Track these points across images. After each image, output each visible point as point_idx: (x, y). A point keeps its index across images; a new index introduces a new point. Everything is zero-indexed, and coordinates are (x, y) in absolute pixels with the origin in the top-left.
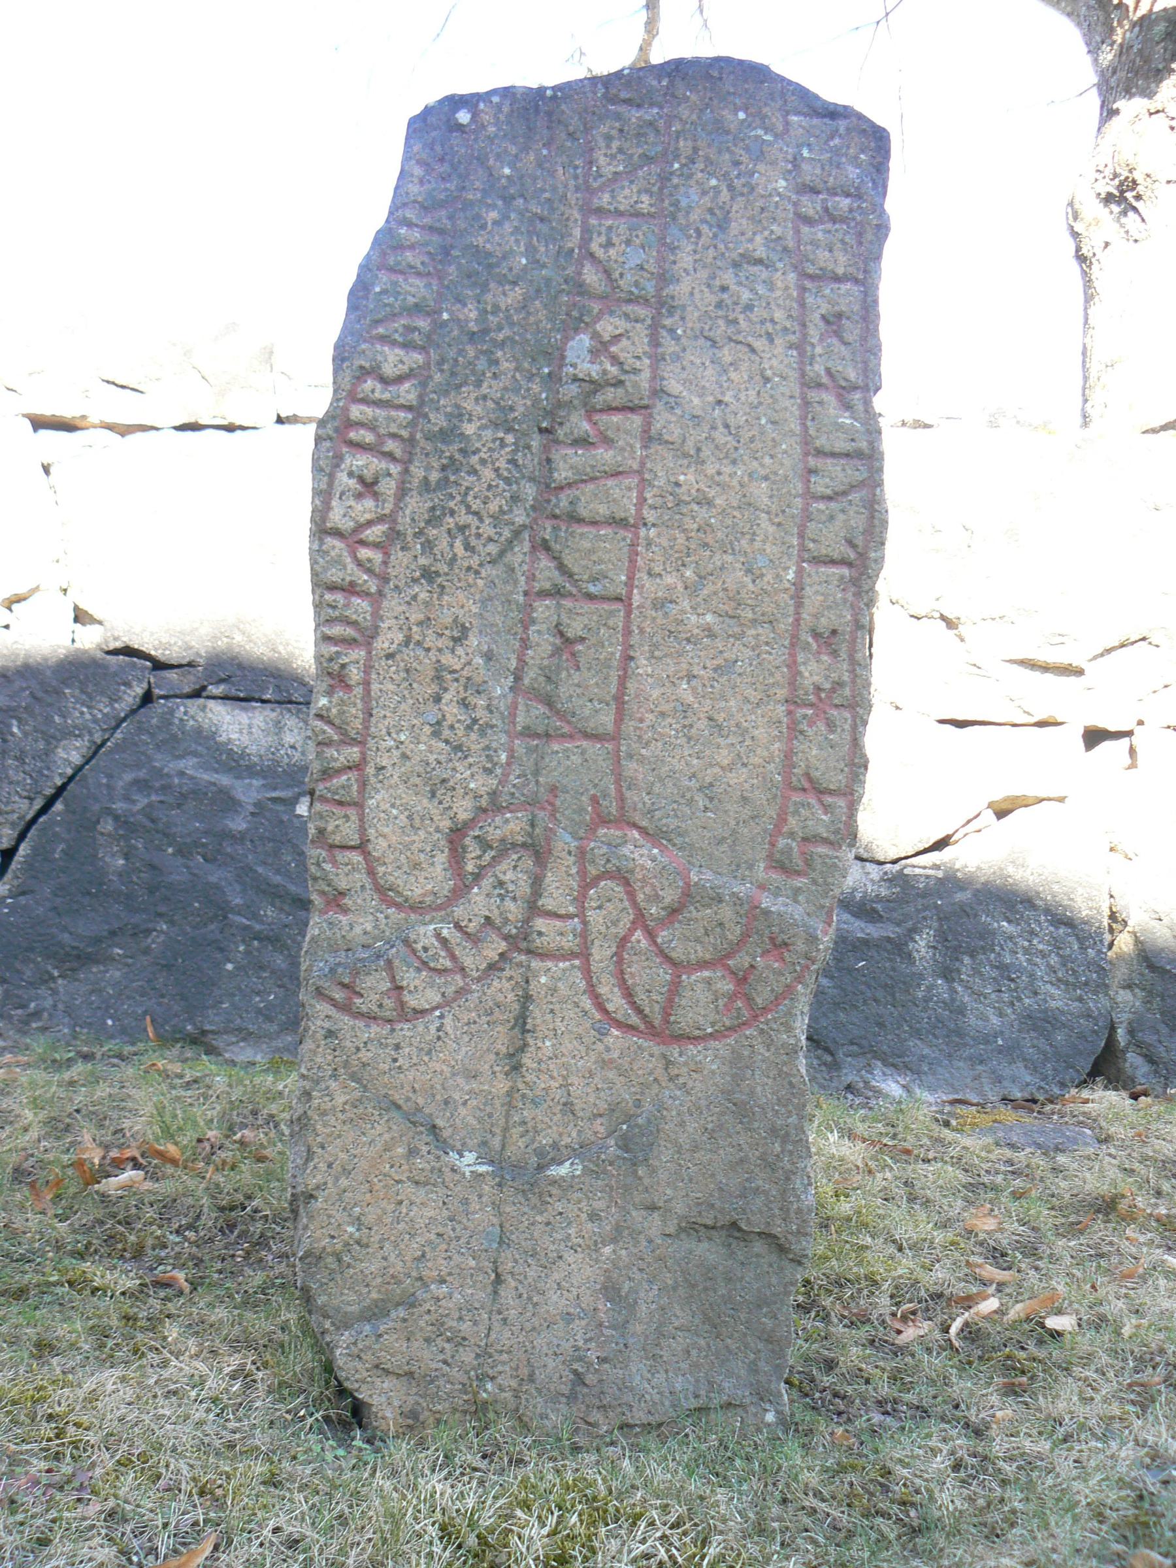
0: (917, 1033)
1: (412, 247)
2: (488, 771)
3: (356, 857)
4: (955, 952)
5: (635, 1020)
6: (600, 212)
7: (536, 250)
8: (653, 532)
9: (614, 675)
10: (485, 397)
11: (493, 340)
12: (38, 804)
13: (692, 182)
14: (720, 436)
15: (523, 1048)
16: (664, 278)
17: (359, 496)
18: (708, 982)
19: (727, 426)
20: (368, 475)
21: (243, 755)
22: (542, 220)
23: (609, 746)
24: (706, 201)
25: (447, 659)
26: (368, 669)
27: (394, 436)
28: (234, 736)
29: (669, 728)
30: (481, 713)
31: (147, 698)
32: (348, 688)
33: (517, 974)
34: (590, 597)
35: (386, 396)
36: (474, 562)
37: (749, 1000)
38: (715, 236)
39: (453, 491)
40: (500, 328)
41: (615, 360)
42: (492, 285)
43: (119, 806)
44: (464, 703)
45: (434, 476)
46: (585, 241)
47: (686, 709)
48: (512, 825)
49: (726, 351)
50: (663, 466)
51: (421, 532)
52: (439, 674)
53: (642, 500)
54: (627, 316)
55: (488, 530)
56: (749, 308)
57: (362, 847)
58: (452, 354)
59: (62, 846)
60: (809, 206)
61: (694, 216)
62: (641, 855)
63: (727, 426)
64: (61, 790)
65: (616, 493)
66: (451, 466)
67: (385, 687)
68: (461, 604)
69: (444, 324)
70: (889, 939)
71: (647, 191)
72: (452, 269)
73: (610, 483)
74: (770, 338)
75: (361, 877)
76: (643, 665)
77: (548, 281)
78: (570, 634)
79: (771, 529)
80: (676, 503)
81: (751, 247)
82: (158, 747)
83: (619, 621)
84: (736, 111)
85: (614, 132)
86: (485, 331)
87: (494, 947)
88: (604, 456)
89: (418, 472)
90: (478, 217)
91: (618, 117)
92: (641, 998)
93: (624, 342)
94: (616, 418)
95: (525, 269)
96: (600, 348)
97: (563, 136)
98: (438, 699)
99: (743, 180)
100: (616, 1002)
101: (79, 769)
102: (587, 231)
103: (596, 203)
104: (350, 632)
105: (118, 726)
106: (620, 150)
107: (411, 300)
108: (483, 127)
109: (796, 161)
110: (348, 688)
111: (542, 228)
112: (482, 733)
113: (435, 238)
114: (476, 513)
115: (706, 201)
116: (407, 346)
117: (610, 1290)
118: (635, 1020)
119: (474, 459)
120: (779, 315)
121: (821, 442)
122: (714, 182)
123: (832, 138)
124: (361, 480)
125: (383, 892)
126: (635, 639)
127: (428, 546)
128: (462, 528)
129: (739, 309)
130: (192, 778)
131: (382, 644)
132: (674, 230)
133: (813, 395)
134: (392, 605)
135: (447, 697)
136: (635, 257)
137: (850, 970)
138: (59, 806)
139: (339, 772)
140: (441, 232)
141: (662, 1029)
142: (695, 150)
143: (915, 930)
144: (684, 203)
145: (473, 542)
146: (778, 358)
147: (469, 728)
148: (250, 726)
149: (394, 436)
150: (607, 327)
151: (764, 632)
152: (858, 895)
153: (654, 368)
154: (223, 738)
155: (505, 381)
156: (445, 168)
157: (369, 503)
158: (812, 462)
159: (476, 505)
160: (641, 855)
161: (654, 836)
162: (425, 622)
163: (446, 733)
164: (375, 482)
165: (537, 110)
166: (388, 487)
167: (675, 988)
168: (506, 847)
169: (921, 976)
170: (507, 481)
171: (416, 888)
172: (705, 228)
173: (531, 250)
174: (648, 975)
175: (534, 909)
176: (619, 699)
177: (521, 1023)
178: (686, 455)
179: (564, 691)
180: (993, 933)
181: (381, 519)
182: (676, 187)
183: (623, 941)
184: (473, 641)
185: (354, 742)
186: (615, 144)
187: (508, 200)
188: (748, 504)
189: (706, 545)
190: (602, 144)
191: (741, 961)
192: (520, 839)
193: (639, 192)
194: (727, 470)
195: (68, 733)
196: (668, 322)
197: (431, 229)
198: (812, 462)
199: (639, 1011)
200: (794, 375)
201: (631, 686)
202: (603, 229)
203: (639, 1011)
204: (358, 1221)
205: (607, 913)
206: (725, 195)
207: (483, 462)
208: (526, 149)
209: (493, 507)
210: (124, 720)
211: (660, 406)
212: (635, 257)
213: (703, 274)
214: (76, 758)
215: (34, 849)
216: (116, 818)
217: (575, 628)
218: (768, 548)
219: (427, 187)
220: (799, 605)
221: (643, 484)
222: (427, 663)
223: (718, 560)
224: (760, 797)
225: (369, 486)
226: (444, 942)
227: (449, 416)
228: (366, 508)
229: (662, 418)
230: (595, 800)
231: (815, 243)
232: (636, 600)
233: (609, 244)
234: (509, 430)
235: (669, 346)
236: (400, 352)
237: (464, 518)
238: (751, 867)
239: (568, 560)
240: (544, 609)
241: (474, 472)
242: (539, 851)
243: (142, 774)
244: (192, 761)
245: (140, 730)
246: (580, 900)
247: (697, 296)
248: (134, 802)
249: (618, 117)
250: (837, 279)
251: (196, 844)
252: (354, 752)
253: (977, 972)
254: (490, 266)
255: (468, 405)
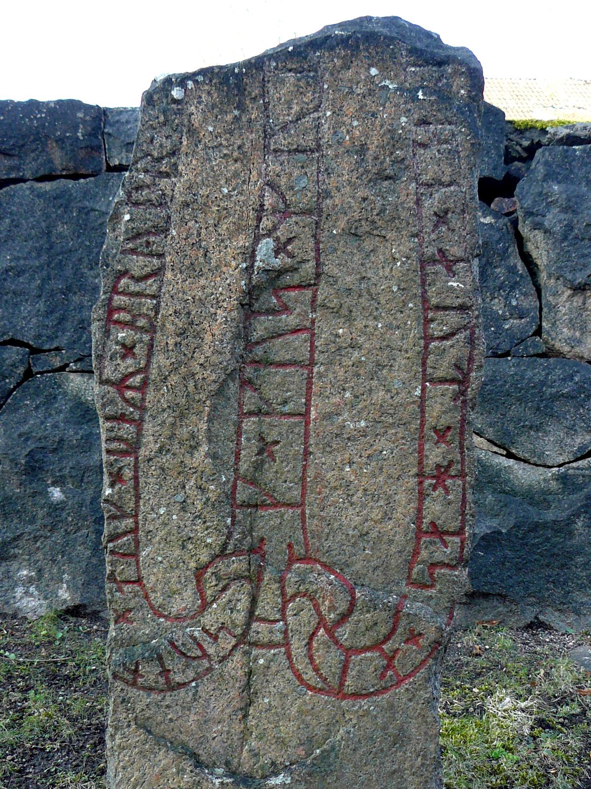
20: (128, 342)
26: (136, 468)
29: (337, 496)
35: (137, 289)
48: (237, 564)
57: (139, 581)
94: (293, 293)
100: (309, 675)
104: (123, 446)
124: (124, 345)
131: (143, 452)
158: (431, 315)
175: (251, 616)
205: (301, 617)
226: (195, 639)
240: (249, 424)
252: (129, 522)
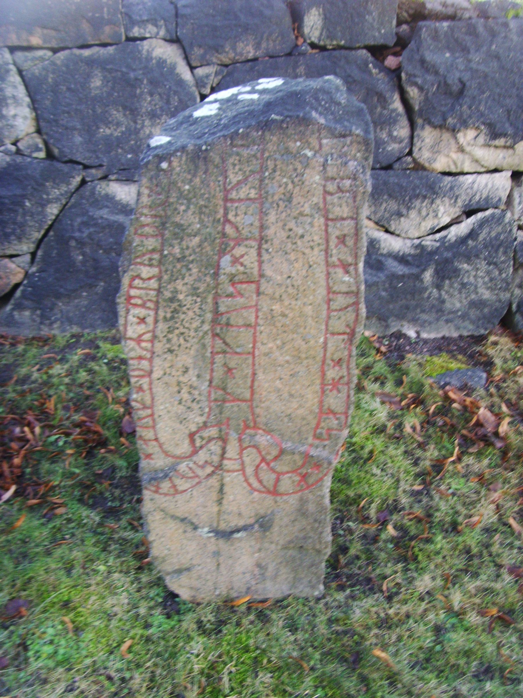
0: (423, 311)
1: (148, 225)
2: (202, 415)
3: (155, 443)
4: (443, 278)
5: (263, 490)
6: (232, 201)
7: (203, 221)
8: (262, 328)
9: (249, 380)
10: (186, 284)
11: (188, 260)
12: (42, 232)
13: (274, 181)
14: (290, 290)
15: (222, 498)
16: (262, 227)
17: (139, 323)
18: (290, 477)
19: (293, 286)
20: (142, 316)
21: (127, 205)
22: (206, 207)
23: (249, 403)
24: (282, 190)
25: (181, 379)
26: (151, 383)
27: (149, 300)
28: (123, 197)
29: (273, 397)
30: (196, 396)
31: (83, 182)
32: (143, 391)
33: (219, 477)
34: (237, 353)
35: (144, 286)
36: (189, 345)
37: (306, 483)
38: (286, 207)
39: (177, 320)
40: (190, 255)
41: (242, 264)
42: (185, 237)
43: (77, 234)
44: (190, 393)
45: (169, 315)
46: (226, 214)
47: (279, 390)
48: (213, 432)
49: (292, 254)
50: (265, 304)
51: (165, 336)
52: (179, 383)
53: (257, 317)
54: (246, 246)
55: (192, 334)
56: (302, 236)
57: (156, 440)
58: (170, 267)
59: (55, 252)
60: (331, 187)
61: (276, 198)
62: (263, 439)
63: (293, 286)
64: (51, 227)
65: (245, 314)
66: (175, 311)
67: (158, 389)
68: (185, 359)
69: (166, 256)
70: (413, 274)
71: (254, 188)
72: (166, 232)
73: (243, 311)
74: (312, 248)
75: (157, 449)
76: (260, 376)
77: (210, 234)
78: (230, 366)
79: (314, 324)
80: (271, 317)
81: (302, 209)
82: (91, 205)
83: (250, 361)
84: (296, 141)
85: (236, 162)
86: (184, 257)
87: (209, 469)
88: (240, 300)
89: (161, 313)
90: (176, 209)
91: (238, 154)
92: (265, 483)
93: (246, 257)
94: (244, 286)
95: (199, 230)
96: (235, 261)
97: (212, 167)
98: (179, 392)
99: (298, 178)
100: (256, 484)
101: (58, 216)
102: (226, 209)
103: (230, 197)
104: (141, 373)
105: (71, 196)
106: (240, 170)
107: (150, 248)
108: (174, 169)
109: (324, 165)
110: (143, 391)
111: (207, 211)
112: (198, 402)
113: (158, 219)
114: (187, 328)
115: (282, 190)
116: (151, 265)
117: (258, 565)
118: (263, 490)
119: (184, 309)
120: (316, 238)
121: (335, 288)
122: (285, 180)
123: (343, 147)
124: (138, 318)
125: (167, 454)
126: (257, 367)
127: (169, 341)
128: (182, 334)
129: (297, 237)
130: (106, 219)
131: (155, 375)
132: (267, 205)
133: (331, 270)
134: (157, 361)
135: (183, 391)
136: (249, 219)
137: (395, 288)
138: (51, 233)
139: (144, 418)
140: (160, 217)
141: (274, 492)
142: (276, 166)
143: (424, 270)
144: (271, 192)
145: (187, 338)
146: (316, 256)
147: (193, 401)
148: (130, 192)
149: (149, 300)
150: (238, 251)
151: (310, 361)
152: (401, 253)
153: (260, 266)
154: (118, 198)
155: (194, 277)
156: (159, 189)
157: (143, 326)
158: (331, 296)
159: (187, 325)
160: (263, 439)
161: (268, 432)
162: (171, 367)
163: (184, 403)
164: (144, 318)
165: (199, 157)
166: (150, 320)
167: (278, 480)
168: (210, 440)
169: (426, 289)
170: (200, 316)
171: (178, 452)
172: (281, 203)
173: (201, 221)
174: (268, 478)
175: (223, 456)
176: (252, 387)
177: (221, 491)
178: (275, 299)
179: (229, 386)
180: (460, 270)
181: (149, 332)
182: (267, 184)
183: (258, 466)
184: (191, 372)
185: (148, 408)
186: (237, 167)
187: (189, 200)
188: (302, 314)
189: (285, 332)
190: (231, 167)
191: (304, 471)
192: (216, 436)
193: (250, 189)
194: (294, 302)
195: (49, 201)
196: (265, 246)
197: (156, 216)
198: (331, 296)
199: (264, 487)
200: (323, 263)
201: (256, 384)
202: (234, 208)
203: (264, 487)
204: (169, 549)
205: (251, 458)
206: (290, 186)
207: (188, 309)
208: (194, 175)
209: (194, 325)
210: (74, 193)
211: (263, 281)
212: (249, 219)
213: (280, 224)
214: (56, 211)
215: (45, 252)
216: (76, 240)
217: (232, 365)
218: (312, 331)
219: (151, 198)
220: (325, 350)
221: (257, 311)
222: (173, 381)
223: (290, 336)
224: (310, 417)
225: (143, 320)
226: (190, 469)
227: (172, 292)
228: (141, 329)
229: (264, 286)
230: (244, 421)
231: (333, 204)
232: (257, 353)
233: (236, 215)
234: (198, 297)
235: (266, 257)
236: (148, 268)
237: (182, 330)
238: (306, 439)
239: (228, 340)
240: (219, 358)
241: (184, 313)
242: (224, 440)
243: (85, 219)
244: (106, 210)
245: (82, 198)
246: (241, 453)
247: (278, 234)
248: (83, 232)
249: (238, 154)
250: (343, 219)
251: (111, 248)
252: (149, 412)
253: (451, 286)
254: (183, 230)
255: (180, 287)
